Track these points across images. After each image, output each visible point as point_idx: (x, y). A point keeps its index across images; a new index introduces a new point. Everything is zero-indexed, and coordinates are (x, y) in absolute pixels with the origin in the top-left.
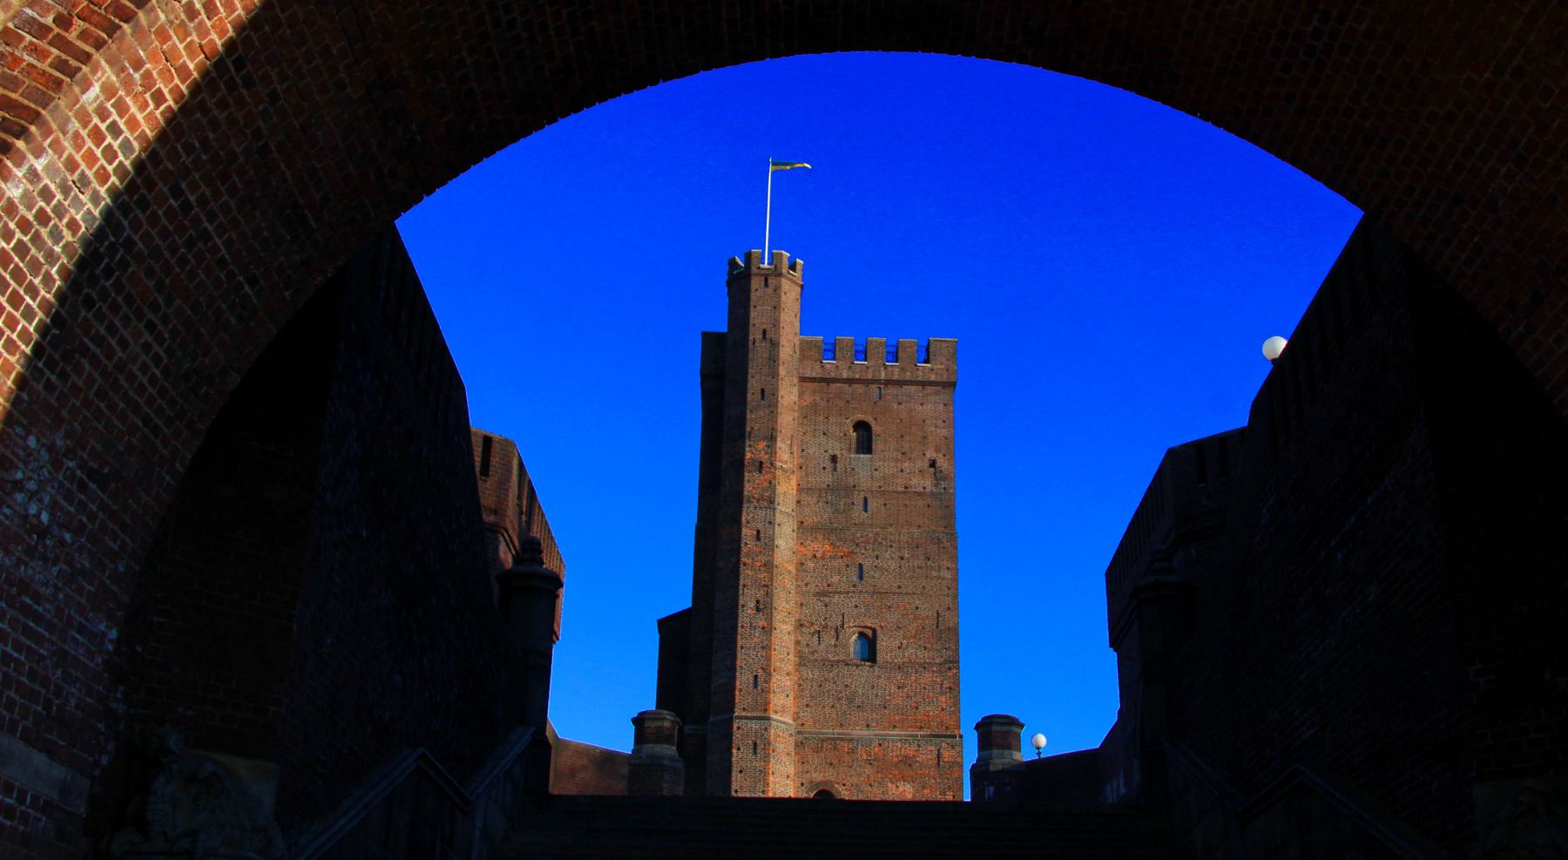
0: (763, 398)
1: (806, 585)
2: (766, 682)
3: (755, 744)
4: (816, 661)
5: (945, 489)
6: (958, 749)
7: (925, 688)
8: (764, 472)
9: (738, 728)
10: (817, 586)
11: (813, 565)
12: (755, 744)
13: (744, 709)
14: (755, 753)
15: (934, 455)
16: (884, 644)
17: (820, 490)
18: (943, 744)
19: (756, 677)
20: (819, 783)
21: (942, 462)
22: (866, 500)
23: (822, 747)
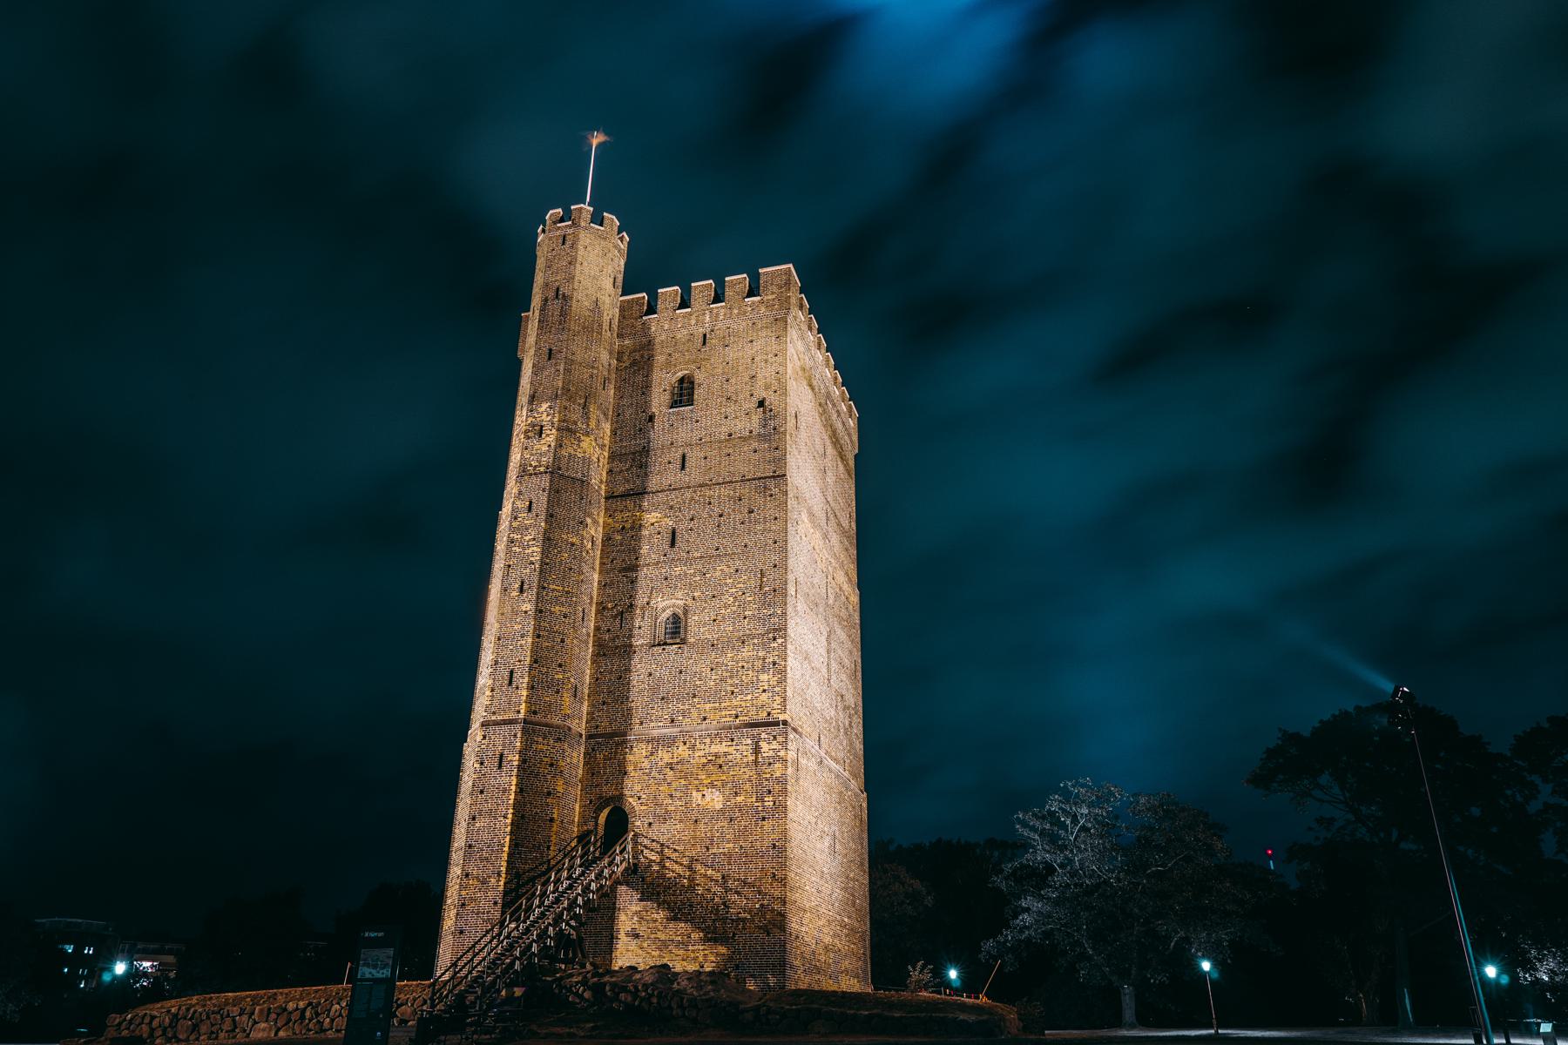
0: (549, 359)
1: (612, 561)
2: (522, 677)
3: (501, 756)
4: (617, 647)
5: (775, 429)
6: (780, 739)
7: (743, 667)
8: (543, 436)
9: (484, 737)
10: (623, 560)
11: (620, 537)
12: (501, 756)
13: (494, 713)
14: (500, 766)
15: (764, 394)
16: (696, 618)
17: (634, 454)
18: (763, 736)
19: (512, 672)
20: (611, 798)
21: (771, 399)
22: (684, 457)
23: (616, 753)
